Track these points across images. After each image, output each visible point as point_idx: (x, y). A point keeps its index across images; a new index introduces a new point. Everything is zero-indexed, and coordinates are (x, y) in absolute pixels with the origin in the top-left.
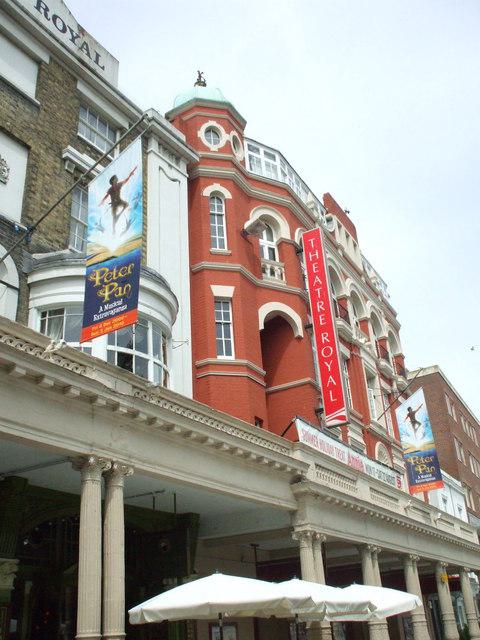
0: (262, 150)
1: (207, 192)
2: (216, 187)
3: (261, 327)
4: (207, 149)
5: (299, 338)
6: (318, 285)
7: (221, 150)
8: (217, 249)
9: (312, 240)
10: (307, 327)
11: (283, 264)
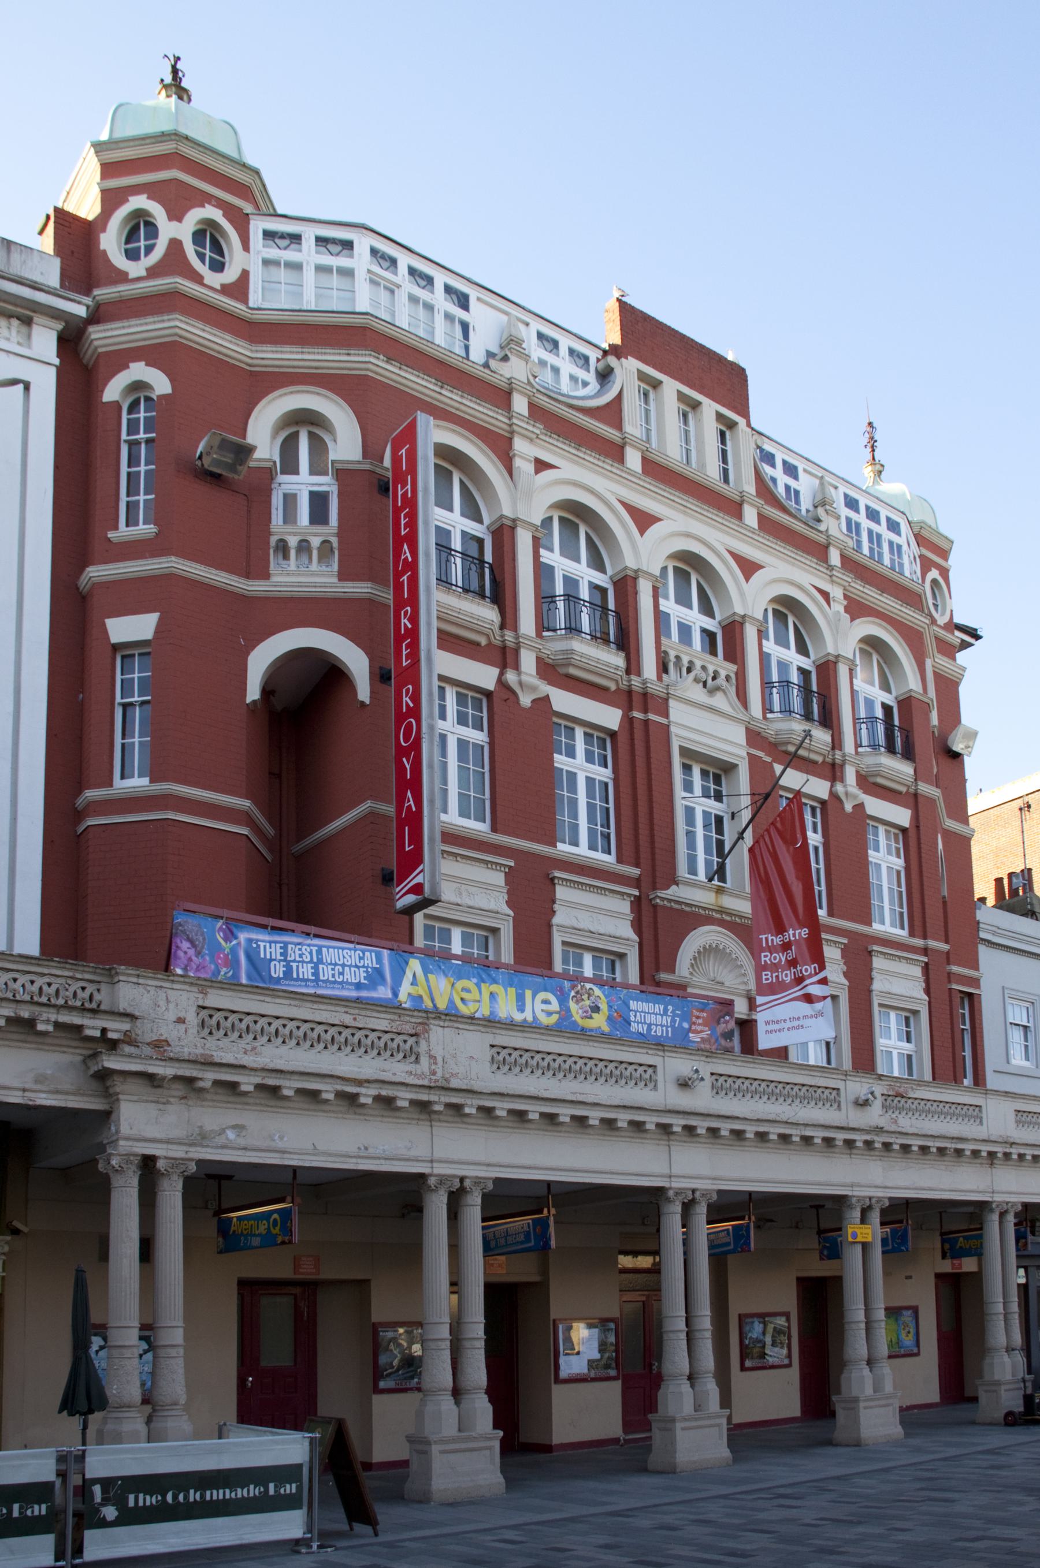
2: (138, 371)
3: (253, 693)
4: (122, 277)
5: (362, 703)
7: (153, 272)
8: (123, 532)
10: (381, 676)
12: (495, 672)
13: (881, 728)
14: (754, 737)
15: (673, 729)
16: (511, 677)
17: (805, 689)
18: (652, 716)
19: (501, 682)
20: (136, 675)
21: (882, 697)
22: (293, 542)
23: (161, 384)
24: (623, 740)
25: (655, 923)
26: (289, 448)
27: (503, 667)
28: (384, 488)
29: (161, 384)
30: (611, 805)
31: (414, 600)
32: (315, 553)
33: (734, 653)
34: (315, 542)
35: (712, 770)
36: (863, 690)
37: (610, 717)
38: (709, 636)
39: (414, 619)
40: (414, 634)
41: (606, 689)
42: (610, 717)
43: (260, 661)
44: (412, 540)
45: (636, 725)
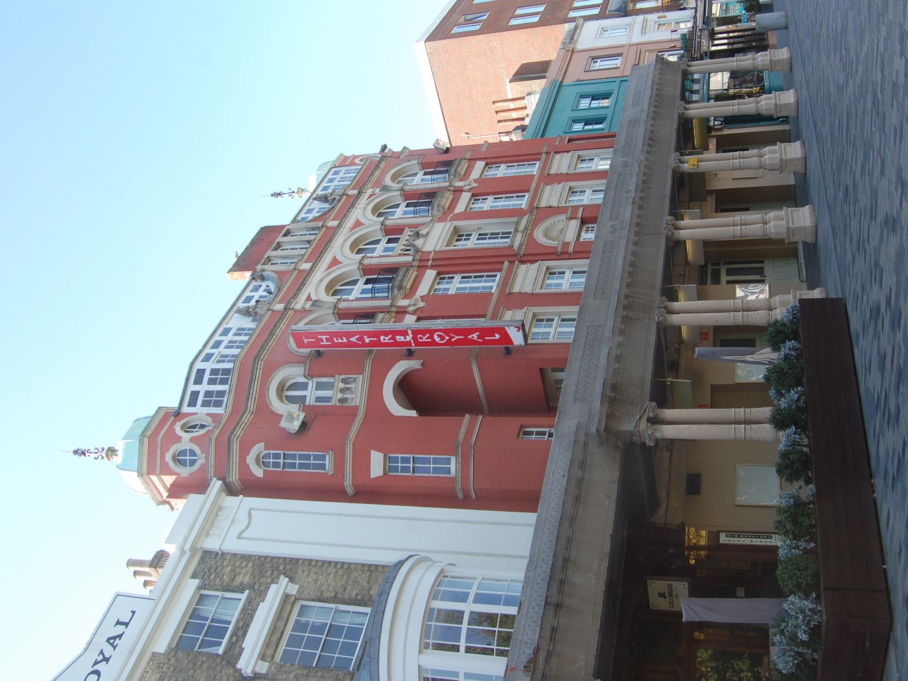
0: (192, 387)
1: (258, 472)
2: (250, 459)
4: (204, 468)
5: (423, 364)
6: (361, 339)
7: (205, 451)
9: (306, 341)
10: (410, 354)
11: (337, 376)
12: (428, 271)
13: (436, 176)
14: (442, 219)
15: (437, 249)
17: (415, 205)
18: (431, 257)
20: (400, 465)
21: (420, 175)
22: (340, 395)
23: (258, 448)
25: (532, 255)
26: (292, 400)
27: (406, 312)
28: (319, 353)
30: (473, 275)
31: (377, 334)
33: (399, 230)
34: (341, 385)
35: (456, 238)
36: (419, 181)
37: (430, 274)
38: (389, 241)
39: (386, 333)
40: (395, 333)
41: (417, 276)
42: (430, 274)
44: (349, 334)
45: (434, 263)
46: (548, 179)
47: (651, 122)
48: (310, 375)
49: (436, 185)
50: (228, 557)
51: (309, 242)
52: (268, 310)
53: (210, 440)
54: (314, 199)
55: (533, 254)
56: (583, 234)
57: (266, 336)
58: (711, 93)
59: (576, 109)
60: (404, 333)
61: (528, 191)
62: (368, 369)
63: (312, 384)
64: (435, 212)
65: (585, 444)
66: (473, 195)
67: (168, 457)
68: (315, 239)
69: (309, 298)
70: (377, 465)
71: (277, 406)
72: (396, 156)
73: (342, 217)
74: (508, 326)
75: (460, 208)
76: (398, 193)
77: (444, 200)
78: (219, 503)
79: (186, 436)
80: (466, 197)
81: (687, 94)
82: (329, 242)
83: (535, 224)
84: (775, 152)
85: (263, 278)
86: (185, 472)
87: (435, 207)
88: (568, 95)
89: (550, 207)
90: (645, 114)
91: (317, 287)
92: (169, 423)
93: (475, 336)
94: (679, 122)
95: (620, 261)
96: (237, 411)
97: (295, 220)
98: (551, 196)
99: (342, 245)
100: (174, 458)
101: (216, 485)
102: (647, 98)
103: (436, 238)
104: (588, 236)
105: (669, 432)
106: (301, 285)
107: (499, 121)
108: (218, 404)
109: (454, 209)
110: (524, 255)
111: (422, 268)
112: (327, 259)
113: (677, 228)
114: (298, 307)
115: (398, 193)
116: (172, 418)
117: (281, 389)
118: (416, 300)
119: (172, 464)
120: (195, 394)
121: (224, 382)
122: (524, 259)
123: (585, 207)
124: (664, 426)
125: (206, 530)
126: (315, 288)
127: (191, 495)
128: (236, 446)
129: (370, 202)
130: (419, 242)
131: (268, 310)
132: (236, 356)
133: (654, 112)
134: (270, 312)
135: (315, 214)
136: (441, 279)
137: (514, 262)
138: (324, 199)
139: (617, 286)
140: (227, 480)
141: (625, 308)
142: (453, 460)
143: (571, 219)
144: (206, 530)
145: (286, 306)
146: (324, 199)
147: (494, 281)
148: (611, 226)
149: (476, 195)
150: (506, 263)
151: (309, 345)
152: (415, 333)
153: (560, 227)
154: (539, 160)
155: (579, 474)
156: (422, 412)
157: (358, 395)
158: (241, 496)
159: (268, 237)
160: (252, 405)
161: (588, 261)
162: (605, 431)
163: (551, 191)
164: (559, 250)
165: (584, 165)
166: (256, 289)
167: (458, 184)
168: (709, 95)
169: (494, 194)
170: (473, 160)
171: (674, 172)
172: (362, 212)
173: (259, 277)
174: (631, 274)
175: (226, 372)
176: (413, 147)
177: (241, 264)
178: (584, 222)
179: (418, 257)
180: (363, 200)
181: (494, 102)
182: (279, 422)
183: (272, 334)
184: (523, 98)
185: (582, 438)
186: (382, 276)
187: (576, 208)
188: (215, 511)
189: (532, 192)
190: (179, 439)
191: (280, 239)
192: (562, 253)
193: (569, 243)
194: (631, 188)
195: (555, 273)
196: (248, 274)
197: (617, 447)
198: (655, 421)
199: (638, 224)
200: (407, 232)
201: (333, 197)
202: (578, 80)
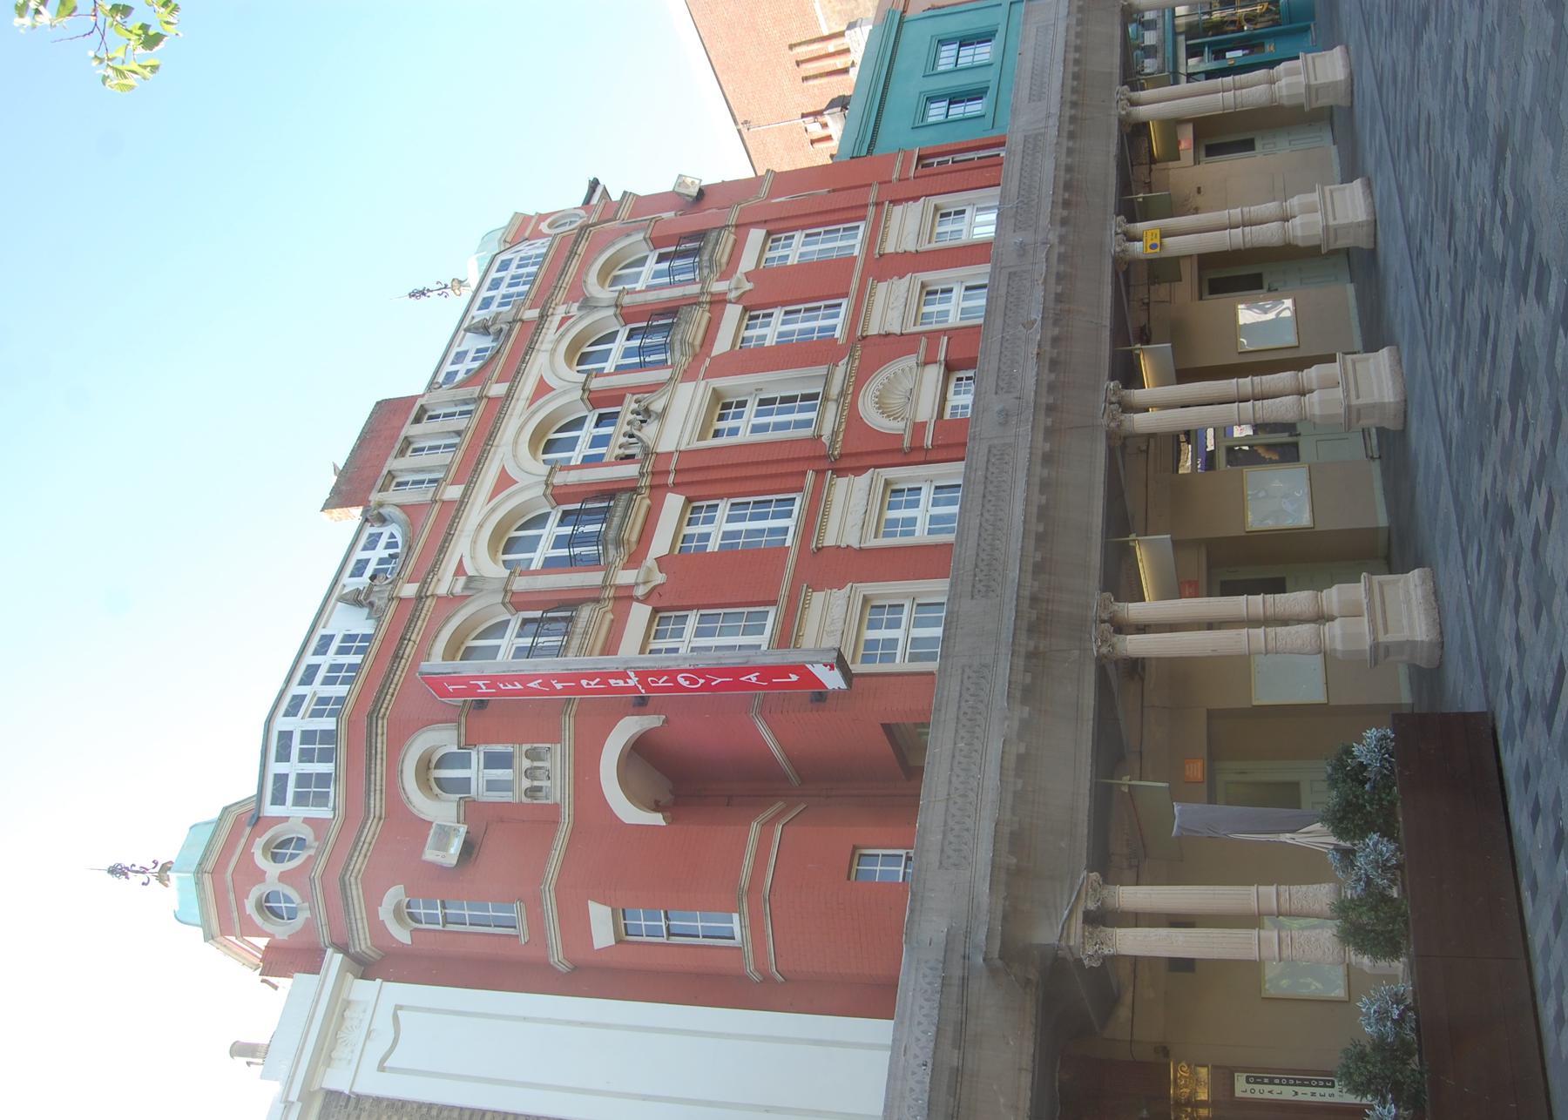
0: (277, 768)
1: (402, 935)
2: (385, 913)
4: (309, 926)
10: (641, 705)
14: (689, 375)
15: (682, 448)
16: (640, 591)
19: (645, 600)
21: (651, 265)
22: (526, 783)
23: (394, 895)
24: (693, 492)
27: (632, 598)
28: (481, 704)
29: (394, 895)
30: (751, 499)
31: (576, 677)
32: (536, 764)
33: (616, 397)
34: (526, 763)
35: (718, 411)
36: (648, 280)
40: (605, 676)
42: (674, 503)
43: (629, 813)
44: (524, 679)
46: (885, 266)
47: (1065, 143)
48: (469, 742)
49: (677, 292)
50: (367, 1106)
51: (459, 433)
52: (391, 599)
53: (312, 880)
54: (467, 330)
55: (862, 452)
56: (950, 394)
57: (388, 664)
58: (1179, 21)
59: (931, 71)
60: (624, 676)
61: (845, 295)
62: (568, 733)
63: (477, 756)
64: (677, 354)
65: (964, 981)
66: (745, 309)
67: (250, 906)
68: (468, 428)
69: (460, 570)
70: (601, 925)
71: (422, 804)
72: (610, 210)
73: (513, 375)
74: (812, 663)
75: (722, 345)
76: (611, 312)
77: (692, 329)
78: (344, 995)
79: (272, 870)
80: (732, 313)
81: (1131, 29)
82: (492, 436)
83: (859, 379)
84: (1296, 72)
85: (382, 520)
86: (282, 931)
87: (677, 346)
88: (917, 37)
89: (888, 335)
90: (1053, 121)
91: (474, 542)
92: (243, 841)
93: (753, 678)
94: (1120, 130)
95: (1018, 508)
96: (355, 814)
97: (432, 385)
98: (890, 308)
99: (516, 442)
100: (260, 907)
101: (334, 960)
102: (1056, 84)
103: (678, 425)
104: (962, 399)
105: (1130, 941)
106: (445, 541)
107: (805, 79)
108: (321, 799)
109: (712, 345)
110: (841, 455)
111: (658, 490)
112: (527, 387)
113: (1129, 408)
114: (442, 590)
115: (611, 312)
116: (248, 830)
117: (425, 765)
118: (649, 570)
119: (257, 919)
120: (281, 779)
121: (325, 757)
122: (842, 465)
123: (952, 333)
124: (1120, 932)
125: (324, 1053)
126: (471, 549)
127: (297, 975)
128: (356, 892)
129: (562, 336)
130: (649, 432)
131: (391, 599)
132: (340, 700)
133: (1073, 119)
134: (395, 603)
135: (470, 364)
136: (752, 318)
137: (824, 471)
138: (483, 329)
139: (1014, 573)
140: (352, 950)
141: (1032, 630)
142: (736, 917)
143: (926, 363)
144: (324, 1053)
145: (420, 590)
146: (483, 329)
147: (789, 514)
148: (1000, 412)
149: (753, 310)
150: (810, 475)
151: (457, 693)
152: (642, 675)
153: (907, 384)
154: (863, 218)
155: (953, 1058)
156: (671, 820)
157: (558, 788)
158: (379, 981)
159: (390, 422)
160: (377, 804)
161: (961, 466)
162: (1001, 958)
163: (889, 293)
164: (906, 444)
165: (948, 227)
166: (372, 544)
167: (718, 287)
168: (1174, 26)
169: (784, 304)
170: (742, 227)
171: (1122, 122)
172: (548, 361)
173: (375, 517)
174: (1041, 539)
175: (328, 736)
176: (643, 190)
177: (340, 497)
178: (950, 368)
179: (649, 467)
180: (550, 333)
181: (791, 47)
182: (422, 851)
183: (397, 657)
184: (841, 34)
185: (957, 972)
186: (590, 505)
187: (933, 336)
188: (339, 1009)
189: (783, 601)
190: (260, 876)
191: (410, 430)
192: (912, 449)
193: (924, 424)
194: (1034, 317)
195: (949, 214)
196: (356, 512)
197: (1028, 981)
198: (1102, 918)
199: (1050, 409)
200: (630, 404)
201: (497, 327)
202: (933, 8)
